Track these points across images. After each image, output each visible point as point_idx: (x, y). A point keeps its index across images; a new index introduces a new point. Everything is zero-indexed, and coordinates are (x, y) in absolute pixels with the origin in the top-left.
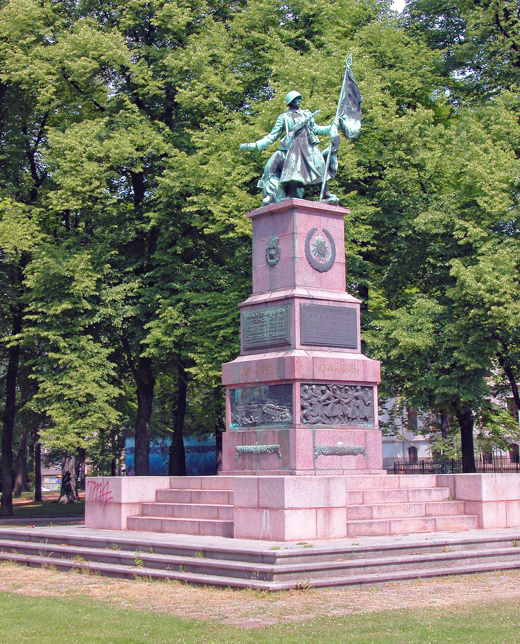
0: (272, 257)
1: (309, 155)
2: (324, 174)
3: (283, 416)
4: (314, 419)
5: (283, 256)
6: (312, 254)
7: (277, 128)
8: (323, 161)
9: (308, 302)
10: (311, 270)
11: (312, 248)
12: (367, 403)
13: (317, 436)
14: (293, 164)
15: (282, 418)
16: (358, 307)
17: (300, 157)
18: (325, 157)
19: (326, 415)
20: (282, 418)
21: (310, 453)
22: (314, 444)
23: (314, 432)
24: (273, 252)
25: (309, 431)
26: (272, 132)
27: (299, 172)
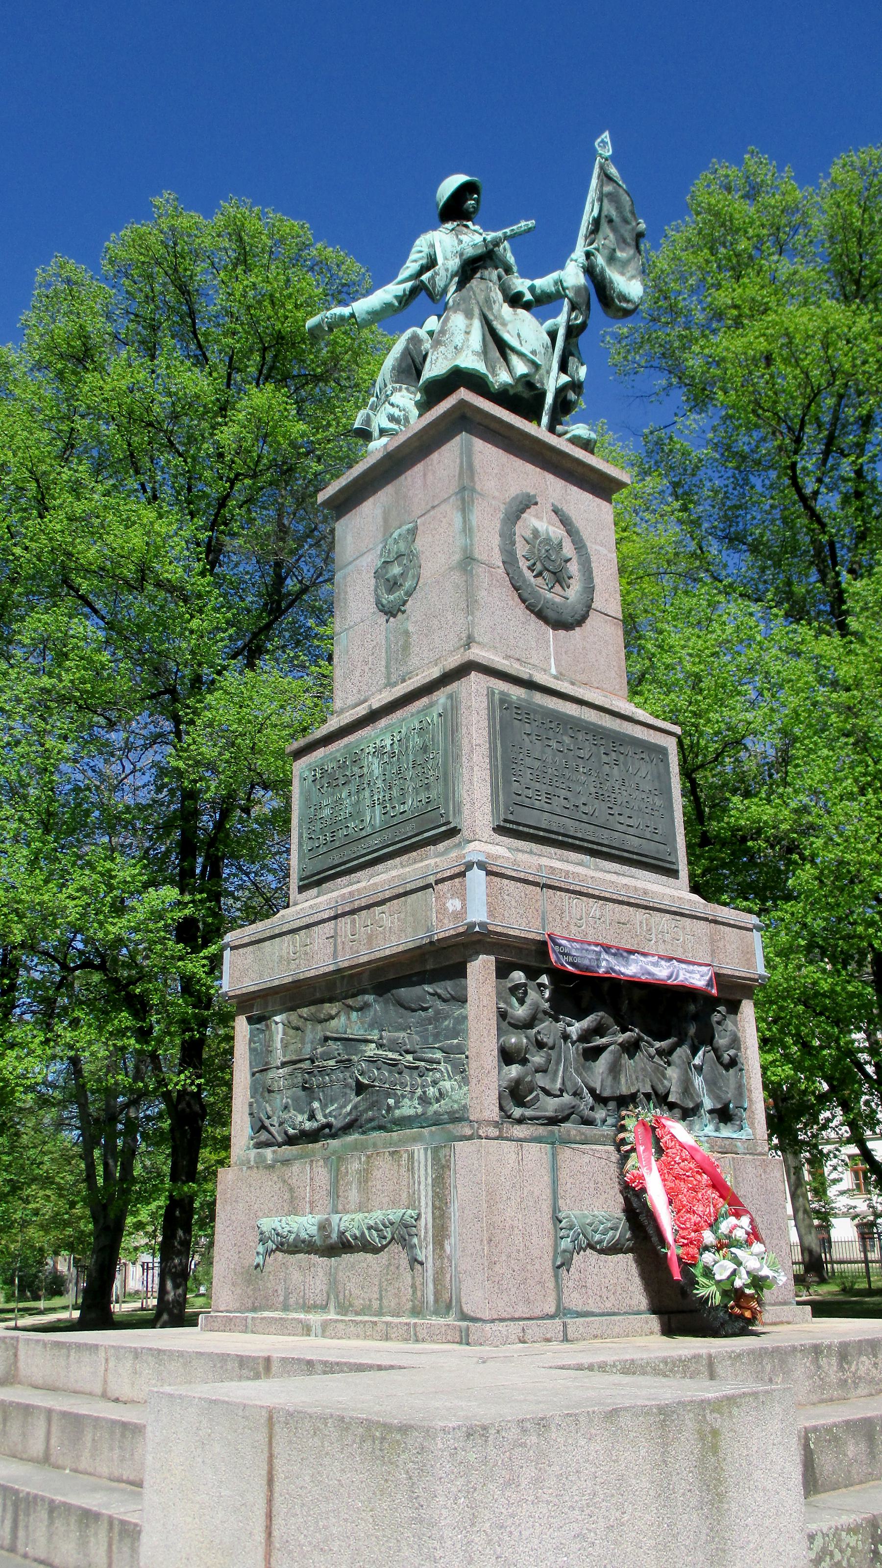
0: (393, 585)
1: (504, 324)
2: (548, 372)
3: (432, 1091)
4: (551, 1106)
5: (425, 573)
6: (523, 564)
7: (411, 267)
8: (547, 339)
9: (517, 693)
10: (520, 610)
11: (521, 549)
12: (726, 1058)
13: (563, 1175)
14: (458, 339)
15: (424, 1100)
16: (671, 744)
17: (477, 324)
18: (553, 335)
19: (592, 1091)
20: (424, 1100)
21: (541, 1244)
22: (555, 1209)
23: (554, 1156)
24: (396, 570)
25: (536, 1153)
26: (401, 277)
27: (475, 353)
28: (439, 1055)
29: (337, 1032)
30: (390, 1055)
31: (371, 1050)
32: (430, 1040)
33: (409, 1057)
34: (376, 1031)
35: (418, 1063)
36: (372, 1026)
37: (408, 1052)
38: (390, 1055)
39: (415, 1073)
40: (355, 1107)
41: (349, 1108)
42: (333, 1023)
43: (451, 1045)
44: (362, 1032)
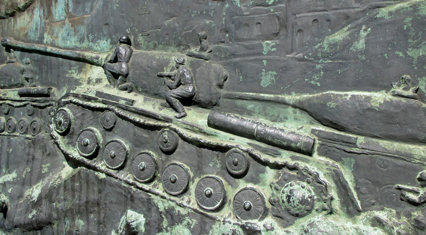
28: (297, 128)
29: (26, 38)
30: (140, 102)
31: (93, 82)
32: (267, 79)
33: (197, 117)
34: (104, 44)
35: (223, 138)
36: (95, 32)
37: (188, 101)
38: (140, 102)
39: (214, 165)
40: (48, 195)
41: (35, 192)
42: (22, 21)
43: (365, 111)
44: (72, 42)
